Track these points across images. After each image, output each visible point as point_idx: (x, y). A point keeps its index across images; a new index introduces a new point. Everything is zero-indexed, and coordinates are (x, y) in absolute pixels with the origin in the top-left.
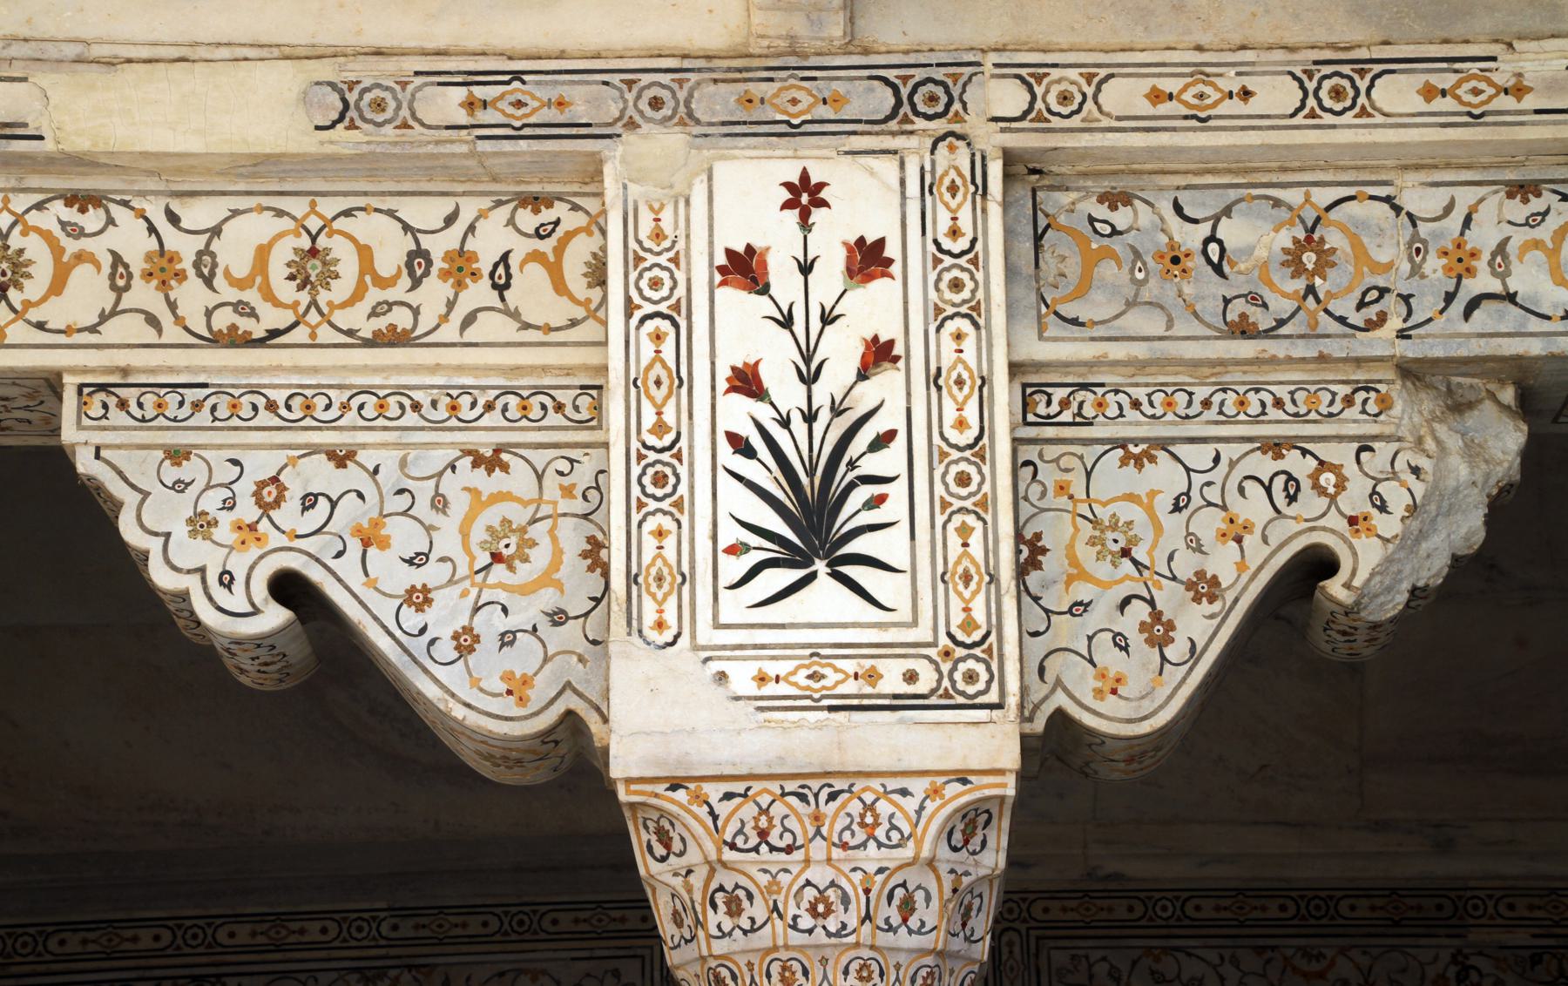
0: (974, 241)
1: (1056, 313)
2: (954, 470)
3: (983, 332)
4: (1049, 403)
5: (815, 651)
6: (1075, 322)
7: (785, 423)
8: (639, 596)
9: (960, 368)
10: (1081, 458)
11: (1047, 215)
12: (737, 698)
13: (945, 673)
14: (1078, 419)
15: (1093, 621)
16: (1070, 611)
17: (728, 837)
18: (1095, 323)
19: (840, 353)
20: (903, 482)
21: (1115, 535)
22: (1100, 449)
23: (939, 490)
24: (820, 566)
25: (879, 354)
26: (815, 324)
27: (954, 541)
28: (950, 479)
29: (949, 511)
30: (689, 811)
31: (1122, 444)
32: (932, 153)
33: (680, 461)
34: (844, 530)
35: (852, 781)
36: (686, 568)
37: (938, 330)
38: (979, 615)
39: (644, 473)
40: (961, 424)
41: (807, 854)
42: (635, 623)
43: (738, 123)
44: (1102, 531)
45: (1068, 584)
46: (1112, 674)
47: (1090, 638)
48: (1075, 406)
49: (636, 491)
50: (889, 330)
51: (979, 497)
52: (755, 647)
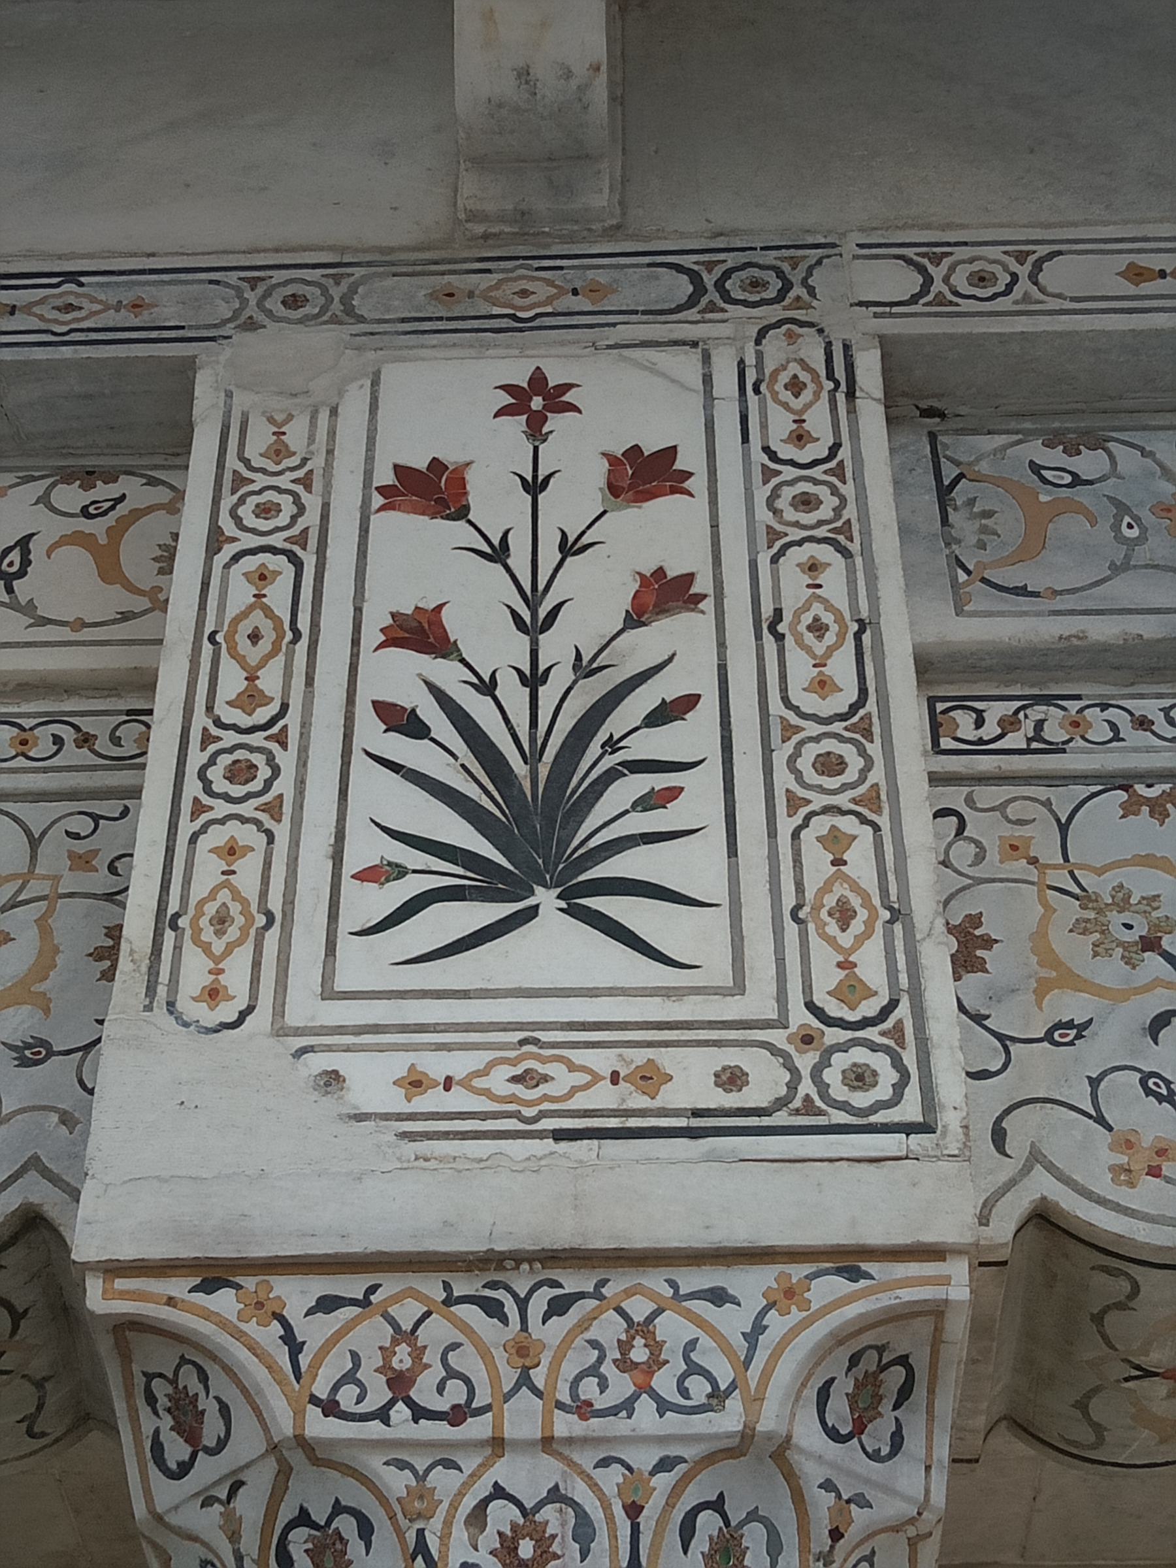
0: (835, 448)
1: (984, 580)
2: (811, 751)
3: (859, 561)
4: (979, 723)
5: (530, 1036)
6: (1022, 591)
7: (488, 687)
8: (178, 948)
9: (817, 609)
10: (1047, 804)
11: (958, 464)
12: (360, 1117)
13: (805, 1073)
14: (1035, 745)
15: (1094, 1054)
16: (1048, 1037)
17: (321, 1390)
18: (1056, 593)
19: (592, 599)
20: (713, 770)
21: (1126, 917)
22: (1083, 791)
23: (783, 779)
24: (546, 898)
25: (662, 594)
26: (549, 555)
27: (817, 862)
28: (805, 764)
29: (803, 811)
30: (239, 1335)
31: (1123, 781)
32: (758, 342)
33: (284, 745)
34: (593, 843)
35: (600, 1274)
36: (275, 903)
37: (775, 560)
38: (871, 966)
39: (212, 761)
40: (823, 685)
41: (498, 1424)
42: (162, 991)
43: (430, 319)
44: (1100, 911)
45: (1040, 993)
46: (1147, 1140)
47: (1094, 1083)
48: (1028, 728)
49: (192, 787)
50: (684, 555)
51: (862, 789)
52: (404, 1029)
